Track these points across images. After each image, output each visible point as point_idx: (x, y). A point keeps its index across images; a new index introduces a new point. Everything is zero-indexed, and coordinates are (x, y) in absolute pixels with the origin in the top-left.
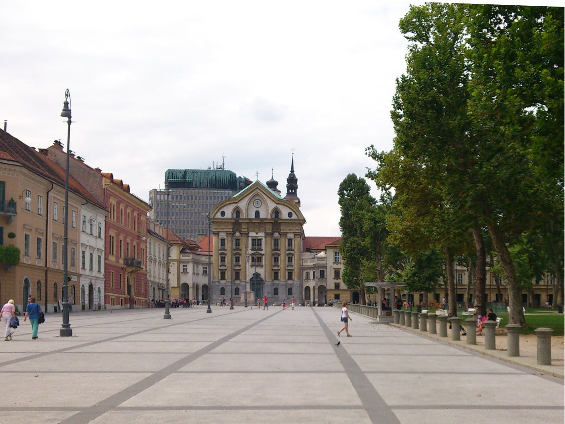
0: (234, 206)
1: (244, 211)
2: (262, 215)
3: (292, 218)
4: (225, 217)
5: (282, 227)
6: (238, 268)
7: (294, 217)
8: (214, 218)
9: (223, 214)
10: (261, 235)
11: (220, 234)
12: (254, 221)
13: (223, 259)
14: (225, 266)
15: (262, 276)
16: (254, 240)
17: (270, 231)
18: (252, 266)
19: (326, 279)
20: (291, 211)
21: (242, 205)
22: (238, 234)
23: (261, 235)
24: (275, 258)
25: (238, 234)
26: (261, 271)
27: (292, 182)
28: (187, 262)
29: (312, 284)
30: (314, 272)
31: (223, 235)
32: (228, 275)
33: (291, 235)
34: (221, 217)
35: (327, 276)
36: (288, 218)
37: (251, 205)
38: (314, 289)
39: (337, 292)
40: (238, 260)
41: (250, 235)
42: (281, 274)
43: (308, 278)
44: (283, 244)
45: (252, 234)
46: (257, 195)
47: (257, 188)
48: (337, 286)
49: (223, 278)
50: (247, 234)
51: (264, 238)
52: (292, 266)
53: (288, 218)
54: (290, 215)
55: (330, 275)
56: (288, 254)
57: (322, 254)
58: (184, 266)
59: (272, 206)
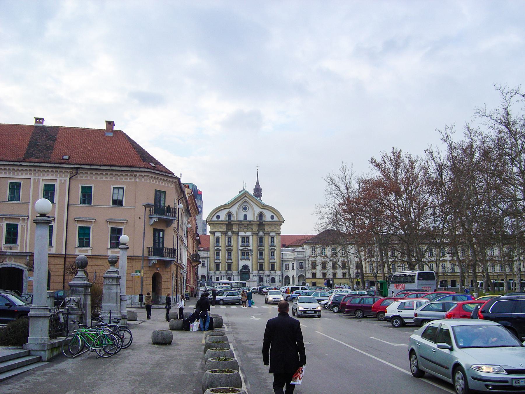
0: (227, 210)
1: (235, 215)
2: (250, 218)
5: (266, 227)
6: (229, 261)
7: (276, 219)
8: (211, 221)
9: (218, 217)
10: (249, 234)
13: (218, 254)
14: (219, 259)
15: (250, 268)
16: (243, 238)
17: (256, 231)
18: (241, 260)
22: (230, 233)
23: (249, 234)
24: (260, 253)
25: (230, 233)
26: (248, 263)
27: (258, 191)
29: (291, 273)
31: (218, 234)
32: (223, 266)
33: (273, 234)
38: (293, 277)
39: (314, 280)
40: (229, 254)
42: (266, 266)
43: (287, 269)
44: (266, 241)
45: (242, 234)
46: (245, 202)
47: (246, 196)
48: (314, 275)
49: (218, 269)
50: (237, 234)
51: (251, 237)
53: (271, 220)
54: (272, 217)
55: (307, 265)
56: (271, 249)
57: (300, 249)
59: (258, 210)
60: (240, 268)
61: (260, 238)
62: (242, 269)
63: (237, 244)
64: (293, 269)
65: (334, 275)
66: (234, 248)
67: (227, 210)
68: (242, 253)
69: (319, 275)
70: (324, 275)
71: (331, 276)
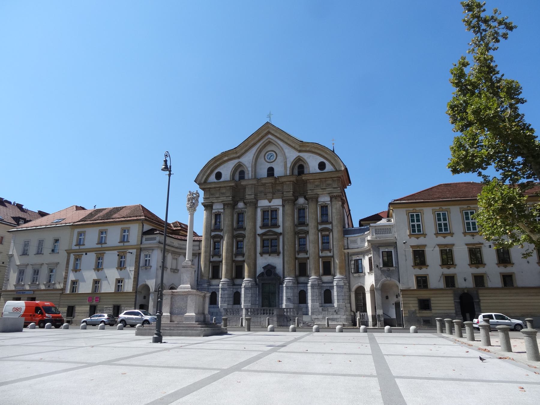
0: (235, 162)
1: (250, 169)
3: (325, 171)
4: (222, 179)
5: (310, 186)
7: (329, 167)
9: (219, 176)
10: (277, 202)
11: (214, 207)
12: (264, 181)
18: (262, 254)
19: (398, 267)
20: (322, 160)
21: (247, 160)
22: (241, 205)
26: (276, 261)
28: (152, 249)
30: (370, 259)
31: (218, 207)
33: (325, 199)
34: (215, 180)
35: (397, 263)
36: (319, 171)
37: (261, 160)
39: (424, 294)
41: (259, 205)
42: (311, 265)
45: (263, 203)
47: (269, 133)
48: (422, 282)
51: (281, 208)
52: (330, 250)
53: (319, 171)
54: (322, 166)
56: (322, 230)
58: (146, 256)
59: (292, 155)
60: (260, 270)
61: (299, 210)
62: (262, 274)
63: (254, 224)
64: (371, 269)
65: (479, 280)
66: (248, 233)
67: (235, 162)
68: (263, 241)
69: (436, 280)
70: (450, 281)
71: (470, 284)
